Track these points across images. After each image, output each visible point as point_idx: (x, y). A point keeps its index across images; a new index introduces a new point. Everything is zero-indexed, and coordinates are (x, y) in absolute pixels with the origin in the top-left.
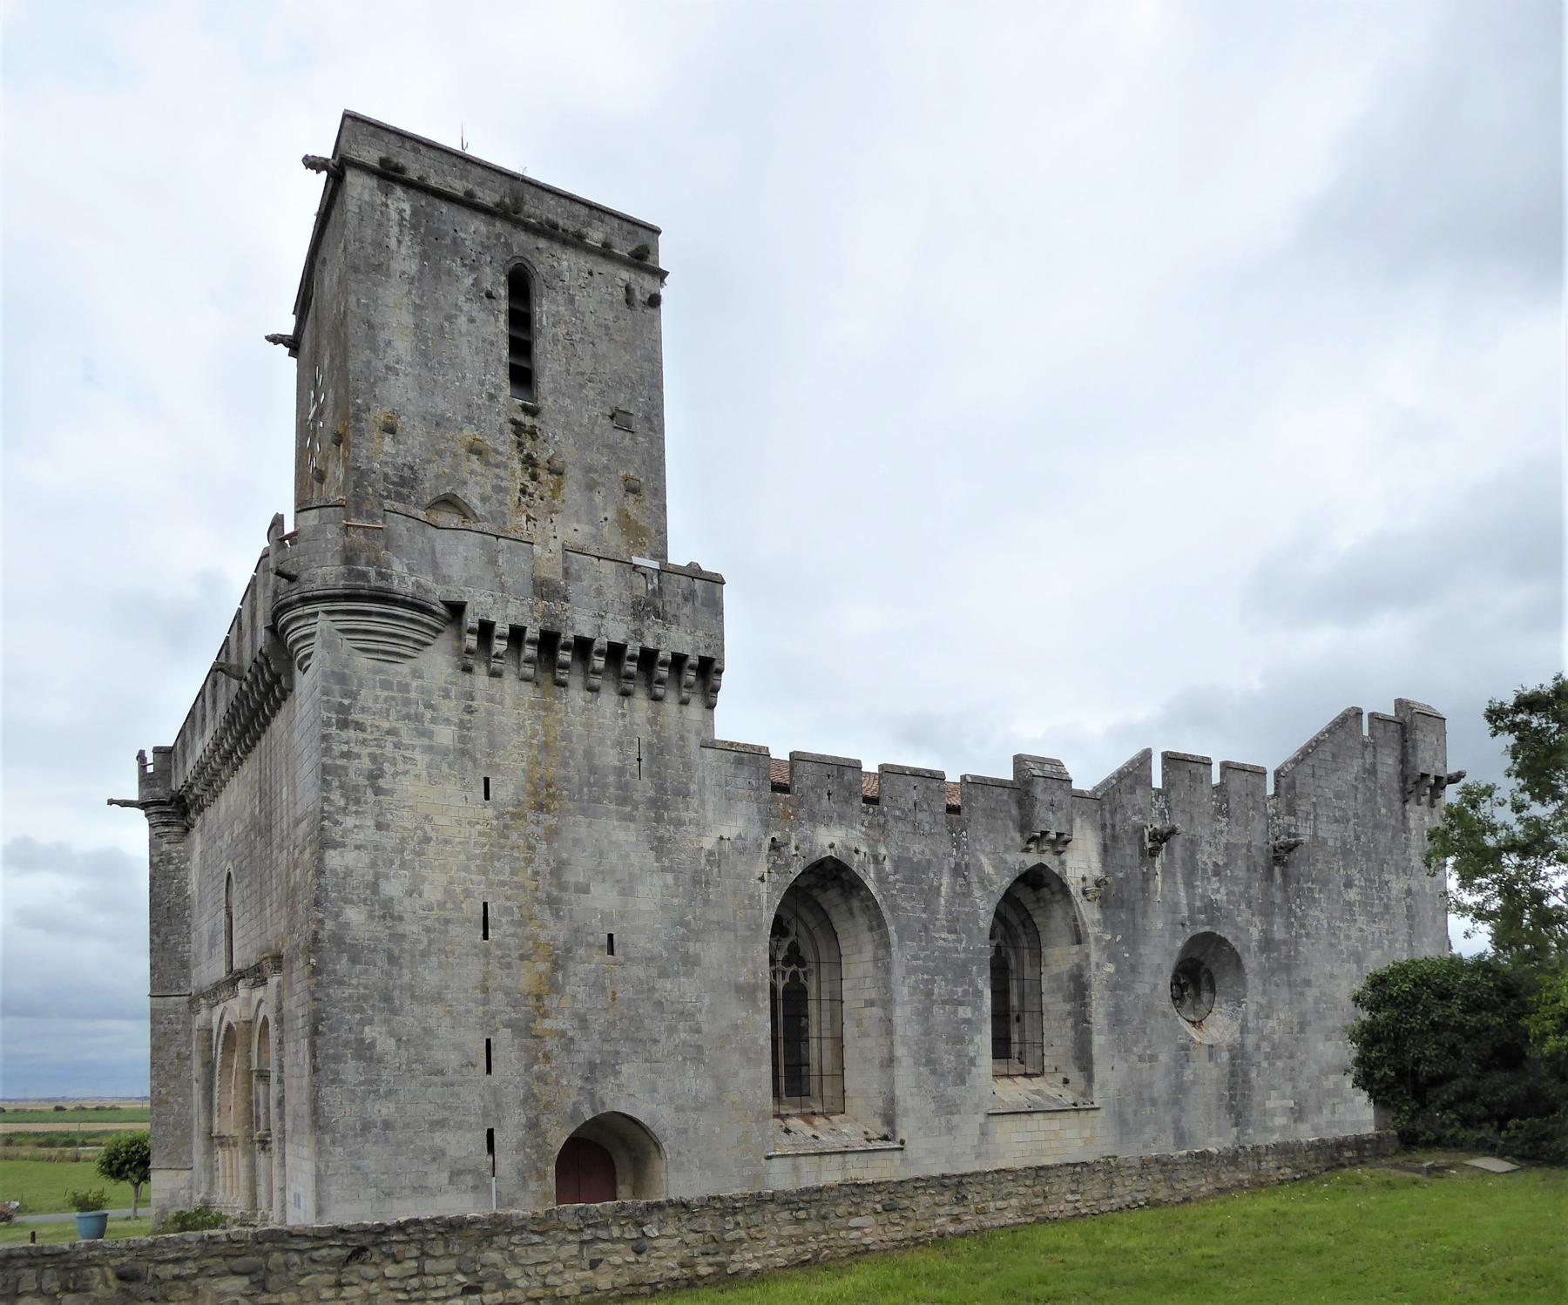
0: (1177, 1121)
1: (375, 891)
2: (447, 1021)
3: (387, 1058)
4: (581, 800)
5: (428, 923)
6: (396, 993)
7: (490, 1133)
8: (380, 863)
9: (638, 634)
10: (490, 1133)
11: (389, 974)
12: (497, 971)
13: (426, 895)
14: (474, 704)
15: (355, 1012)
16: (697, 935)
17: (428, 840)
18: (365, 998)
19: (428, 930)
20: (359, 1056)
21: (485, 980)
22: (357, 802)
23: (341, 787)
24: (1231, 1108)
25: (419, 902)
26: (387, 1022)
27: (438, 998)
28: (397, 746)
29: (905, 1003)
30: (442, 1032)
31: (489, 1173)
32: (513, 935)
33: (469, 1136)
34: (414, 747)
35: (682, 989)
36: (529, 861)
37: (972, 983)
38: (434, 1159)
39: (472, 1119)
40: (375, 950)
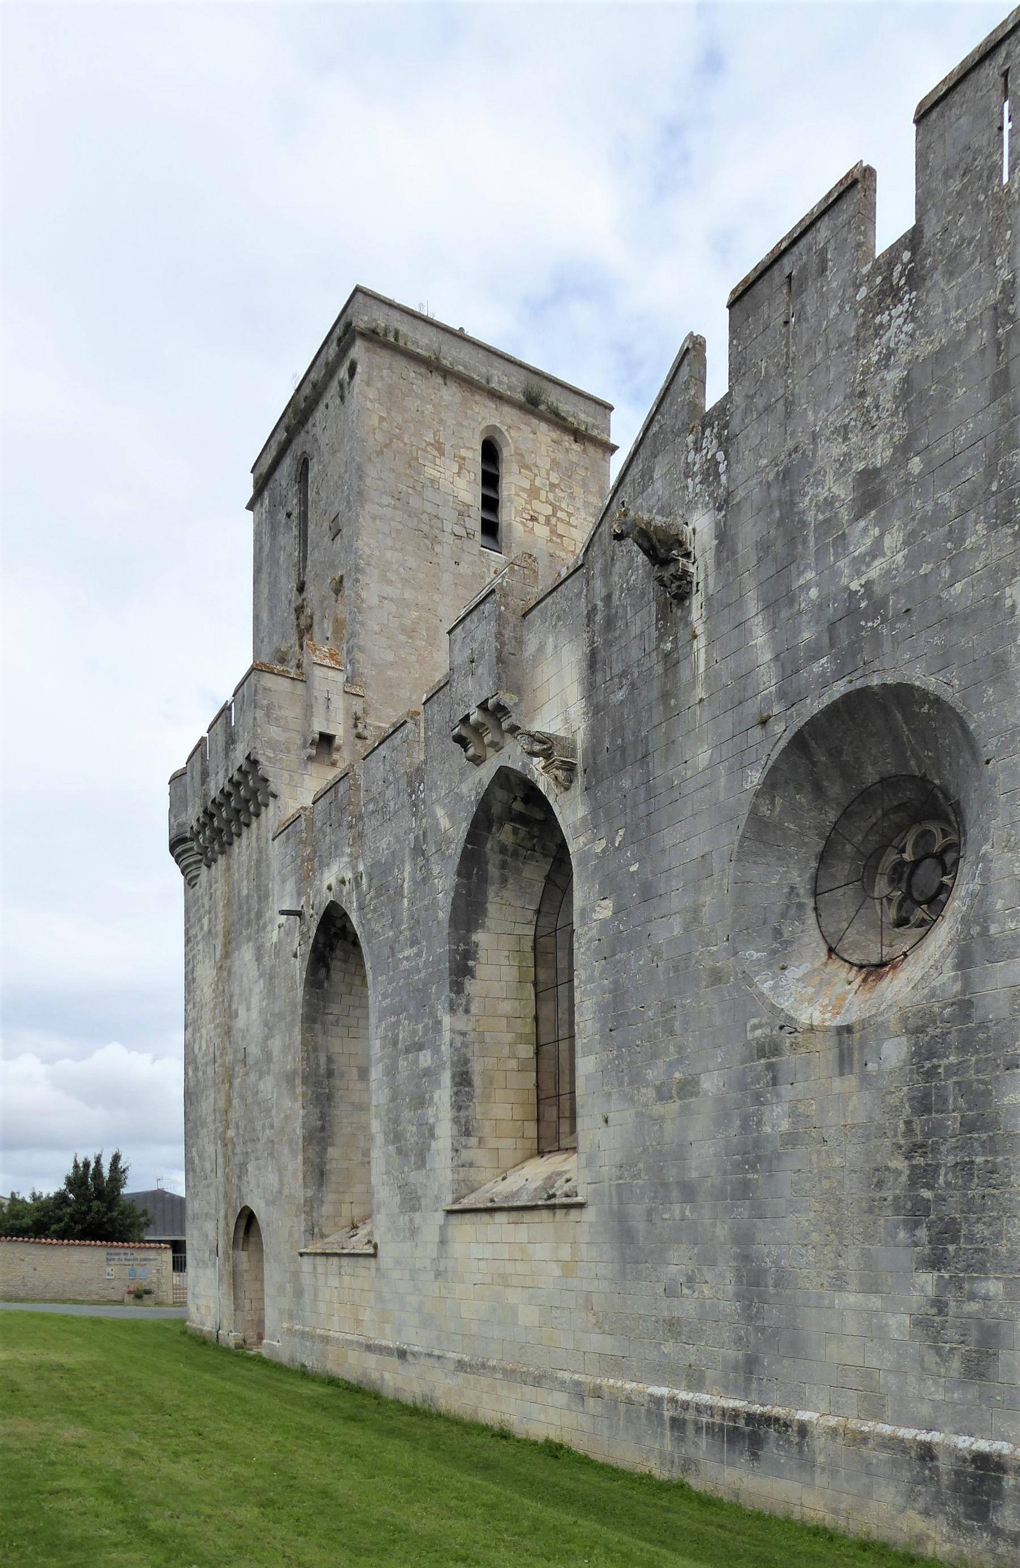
0: (744, 1239)
24: (916, 1213)
29: (380, 1060)
37: (432, 1014)
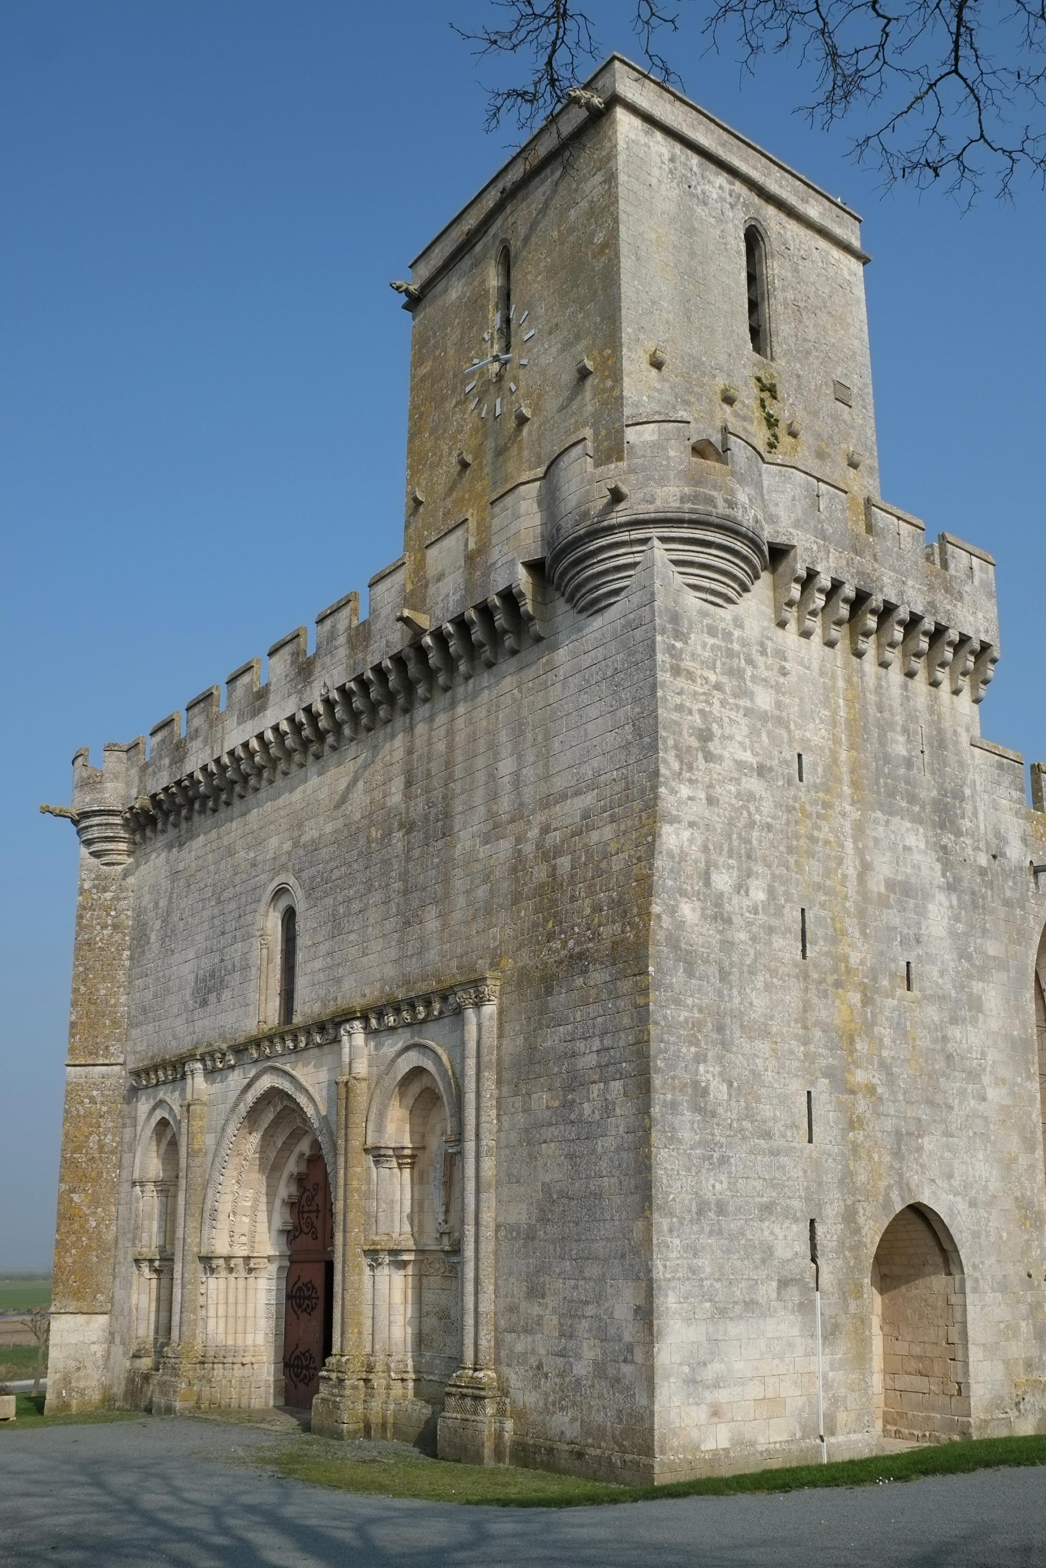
1: (707, 883)
2: (772, 1063)
3: (720, 1110)
4: (878, 793)
5: (755, 929)
6: (728, 1020)
7: (812, 1222)
8: (711, 847)
9: (932, 605)
10: (812, 1222)
11: (721, 995)
12: (815, 1000)
13: (752, 893)
14: (787, 665)
15: (691, 1044)
16: (982, 973)
17: (752, 824)
18: (698, 1025)
19: (754, 939)
20: (697, 1109)
21: (805, 1011)
22: (690, 769)
23: (676, 747)
25: (747, 902)
26: (720, 1059)
27: (765, 1033)
28: (723, 703)
30: (769, 1076)
31: (813, 1285)
32: (828, 954)
33: (794, 1227)
34: (738, 707)
35: (969, 1038)
36: (840, 861)
38: (763, 1261)
39: (796, 1204)
40: (707, 961)
